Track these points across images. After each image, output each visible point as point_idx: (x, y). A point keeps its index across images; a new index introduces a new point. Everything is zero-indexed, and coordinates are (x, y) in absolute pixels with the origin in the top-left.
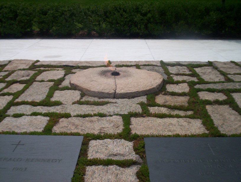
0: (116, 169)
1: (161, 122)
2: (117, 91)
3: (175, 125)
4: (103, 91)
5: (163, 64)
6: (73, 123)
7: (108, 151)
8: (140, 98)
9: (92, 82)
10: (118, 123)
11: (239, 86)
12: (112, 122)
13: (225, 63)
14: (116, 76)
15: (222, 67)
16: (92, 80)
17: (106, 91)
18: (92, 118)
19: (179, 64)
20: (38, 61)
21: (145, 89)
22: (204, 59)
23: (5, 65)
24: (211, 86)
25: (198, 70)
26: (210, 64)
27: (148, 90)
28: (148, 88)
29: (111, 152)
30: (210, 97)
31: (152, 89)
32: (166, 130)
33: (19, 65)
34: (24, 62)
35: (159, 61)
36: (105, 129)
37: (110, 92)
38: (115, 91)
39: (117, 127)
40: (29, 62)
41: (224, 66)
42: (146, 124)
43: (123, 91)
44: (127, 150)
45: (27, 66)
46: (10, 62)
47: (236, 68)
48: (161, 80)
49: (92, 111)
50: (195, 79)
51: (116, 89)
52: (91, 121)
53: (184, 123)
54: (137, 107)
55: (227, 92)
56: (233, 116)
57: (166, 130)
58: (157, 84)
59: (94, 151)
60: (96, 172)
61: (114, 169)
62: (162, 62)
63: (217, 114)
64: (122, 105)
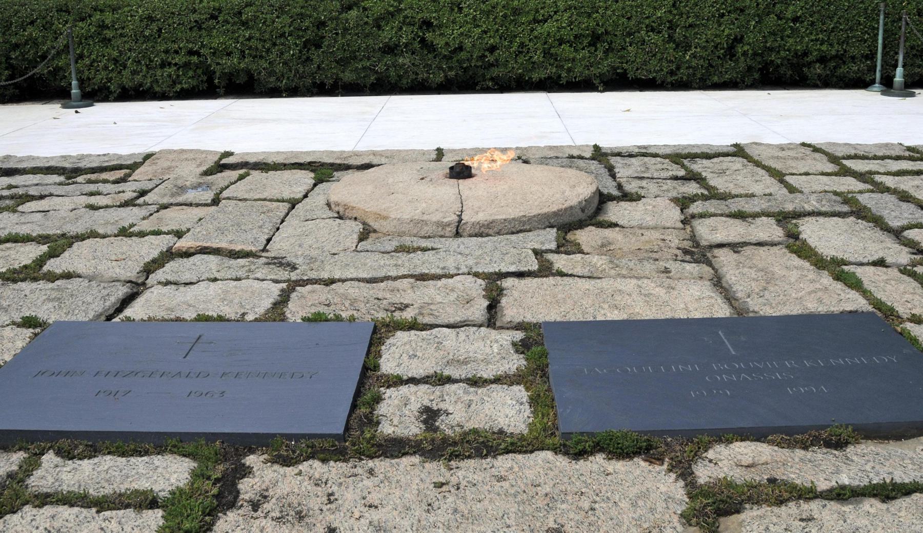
0: (468, 393)
1: (591, 288)
2: (465, 218)
3: (630, 295)
4: (425, 217)
5: (599, 154)
6: (343, 295)
7: (442, 353)
8: (530, 234)
9: (392, 197)
10: (469, 293)
11: (819, 201)
12: (452, 290)
13: (782, 148)
14: (461, 181)
15: (773, 157)
16: (392, 191)
17: (436, 217)
18: (398, 284)
19: (644, 153)
20: (228, 154)
21: (545, 210)
22: (723, 139)
23: (134, 167)
24: (735, 205)
25: (698, 166)
26: (739, 151)
27: (554, 212)
28: (555, 208)
29: (451, 354)
30: (733, 231)
31: (566, 209)
32: (606, 306)
33: (174, 164)
34: (192, 156)
35: (587, 146)
36: (432, 307)
37: (445, 220)
38: (460, 216)
39: (468, 303)
40: (204, 156)
41: (781, 154)
42: (548, 292)
43: (482, 217)
44: (496, 350)
45: (199, 166)
46: (148, 156)
47: (815, 159)
48: (593, 188)
49: (394, 268)
50: (692, 188)
51: (462, 212)
52: (392, 291)
53: (657, 289)
54: (523, 255)
55: (783, 218)
56: (795, 272)
57: (606, 306)
58: (582, 197)
59: (404, 355)
60: (412, 401)
61: (461, 392)
62: (596, 148)
63: (750, 268)
64: (480, 252)
